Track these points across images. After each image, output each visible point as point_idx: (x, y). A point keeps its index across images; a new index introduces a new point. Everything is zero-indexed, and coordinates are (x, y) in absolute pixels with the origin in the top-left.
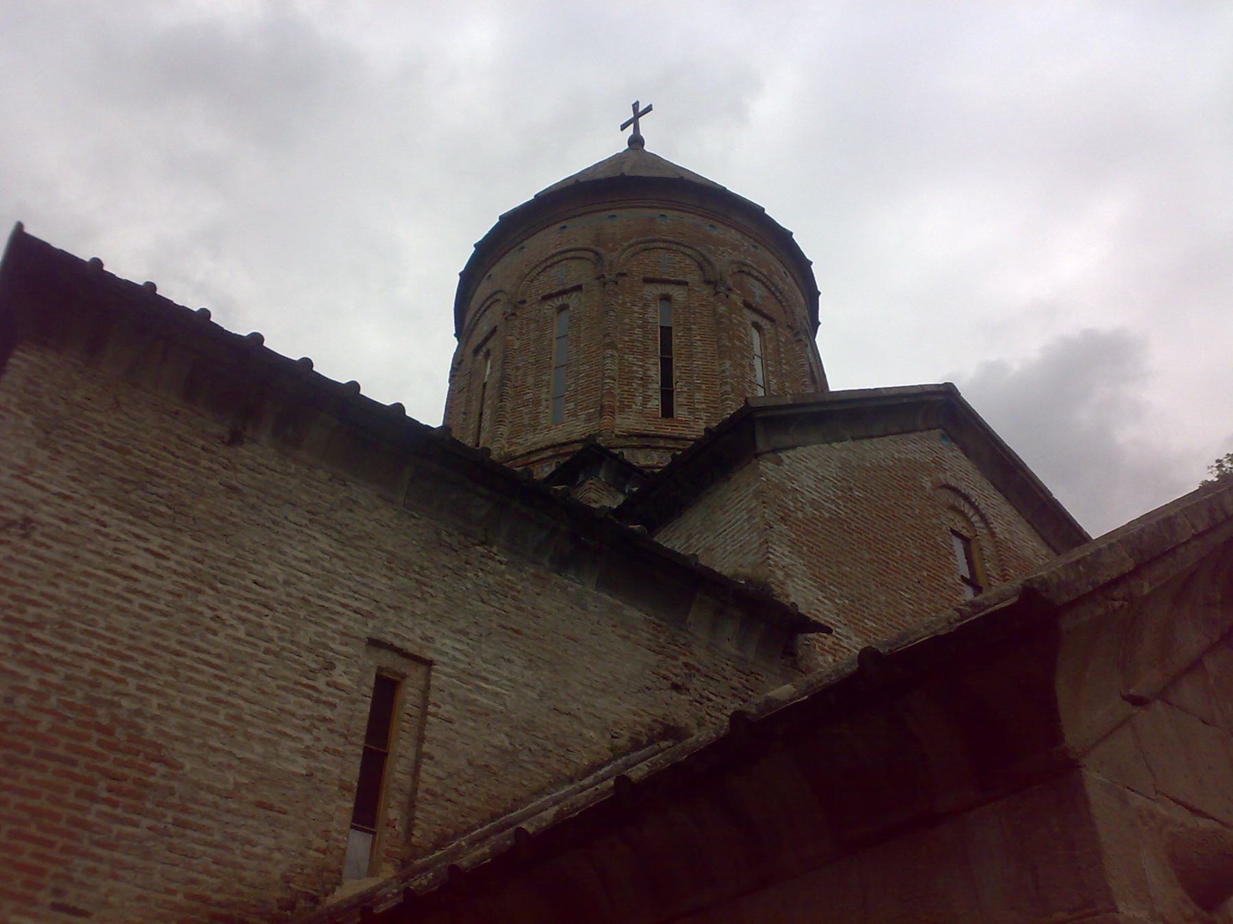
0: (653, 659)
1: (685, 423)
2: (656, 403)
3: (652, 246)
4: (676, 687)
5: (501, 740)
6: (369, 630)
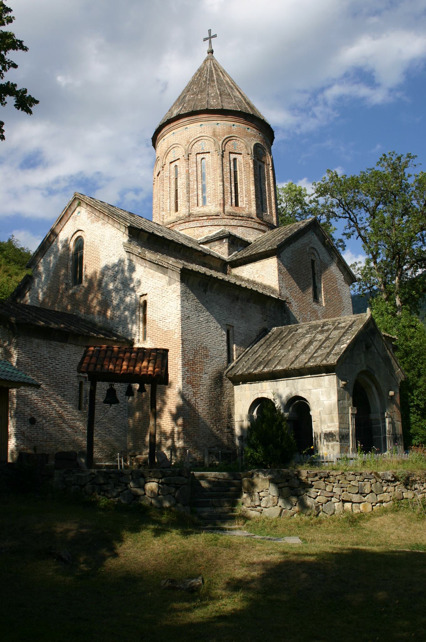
0: (261, 316)
1: (243, 209)
2: (234, 201)
3: (231, 138)
4: (265, 321)
5: (243, 338)
6: (225, 323)
